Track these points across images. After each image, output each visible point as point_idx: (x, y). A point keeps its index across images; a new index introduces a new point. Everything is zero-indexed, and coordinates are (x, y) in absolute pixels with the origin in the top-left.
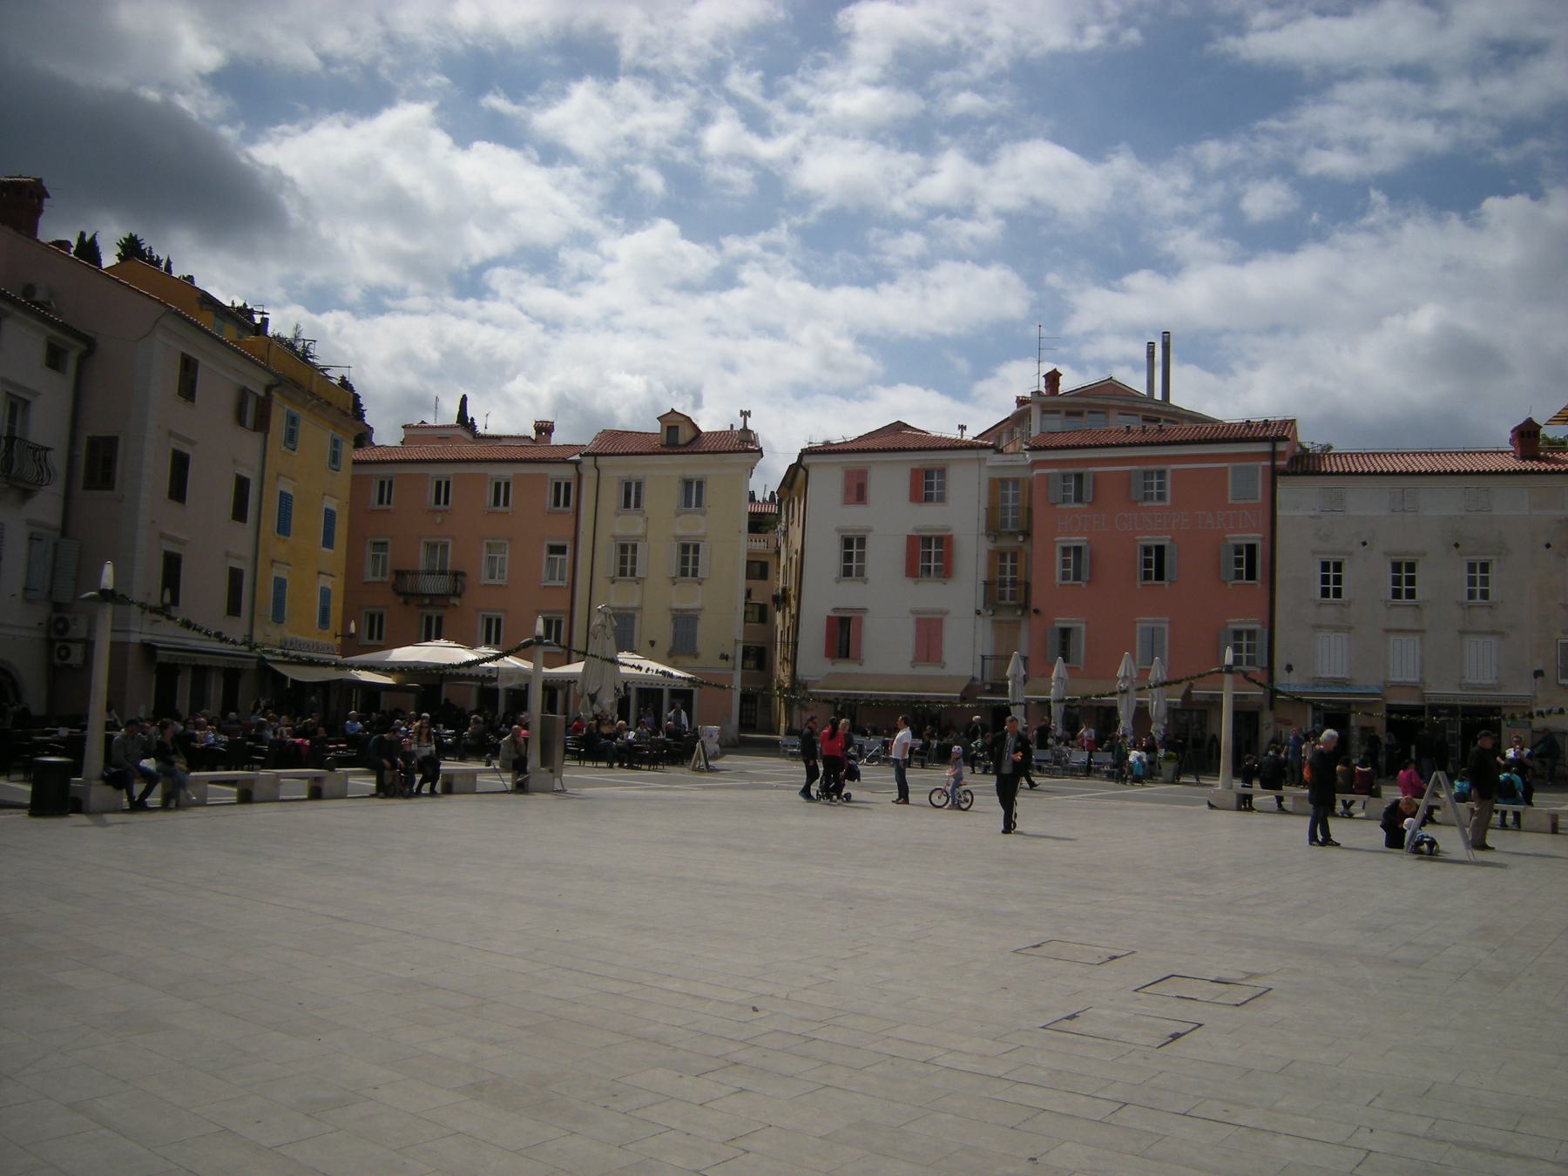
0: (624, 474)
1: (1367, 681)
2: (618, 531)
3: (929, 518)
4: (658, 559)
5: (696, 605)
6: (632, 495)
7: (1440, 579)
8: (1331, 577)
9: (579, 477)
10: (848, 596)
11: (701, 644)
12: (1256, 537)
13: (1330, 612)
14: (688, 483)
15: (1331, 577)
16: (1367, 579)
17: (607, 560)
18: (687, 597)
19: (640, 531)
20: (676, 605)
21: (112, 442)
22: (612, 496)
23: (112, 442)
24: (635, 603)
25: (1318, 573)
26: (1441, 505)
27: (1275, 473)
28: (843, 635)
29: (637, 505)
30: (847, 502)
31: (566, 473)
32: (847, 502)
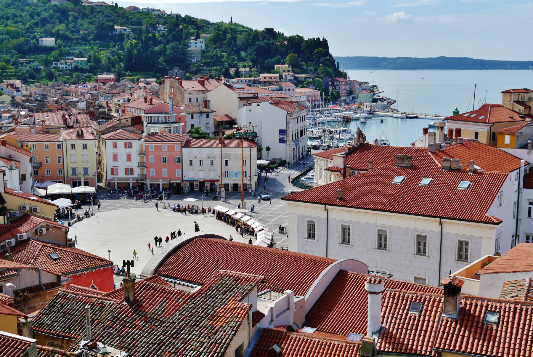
0: (72, 143)
1: (196, 178)
6: (73, 147)
7: (206, 163)
8: (191, 162)
10: (115, 164)
11: (89, 173)
12: (180, 157)
13: (191, 167)
15: (191, 162)
16: (196, 162)
18: (86, 165)
20: (84, 166)
21: (25, 175)
22: (69, 147)
23: (25, 175)
26: (206, 151)
27: (182, 147)
28: (114, 171)
31: (60, 143)
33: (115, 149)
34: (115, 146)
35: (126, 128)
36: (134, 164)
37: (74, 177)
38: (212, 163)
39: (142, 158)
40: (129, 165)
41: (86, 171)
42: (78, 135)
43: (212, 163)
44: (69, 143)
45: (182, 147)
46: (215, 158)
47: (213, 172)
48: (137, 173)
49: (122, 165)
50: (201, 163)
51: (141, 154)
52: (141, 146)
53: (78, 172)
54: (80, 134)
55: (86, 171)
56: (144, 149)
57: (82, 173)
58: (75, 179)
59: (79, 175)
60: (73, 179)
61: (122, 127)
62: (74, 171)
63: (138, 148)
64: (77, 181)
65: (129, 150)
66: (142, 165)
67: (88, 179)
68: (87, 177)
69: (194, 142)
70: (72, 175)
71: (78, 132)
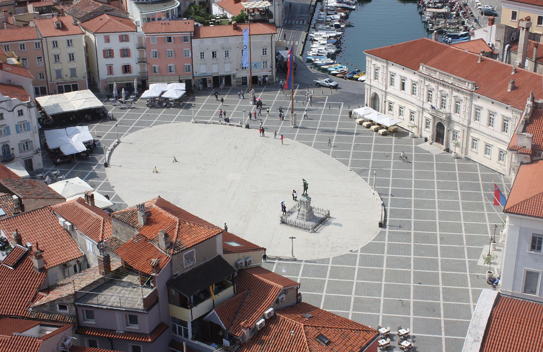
0: (53, 40)
1: (209, 73)
2: (54, 53)
3: (125, 45)
4: (64, 58)
5: (75, 67)
7: (220, 54)
8: (202, 55)
9: (42, 41)
11: (77, 74)
13: (202, 61)
14: (68, 41)
15: (202, 55)
17: (52, 59)
18: (72, 65)
19: (59, 52)
20: (70, 67)
22: (51, 45)
24: (61, 68)
25: (200, 55)
26: (220, 41)
27: (191, 38)
29: (57, 46)
30: (106, 42)
32: (106, 42)
33: (108, 44)
34: (107, 40)
35: (111, 13)
36: (132, 61)
37: (59, 81)
38: (227, 54)
39: (141, 53)
40: (126, 61)
41: (73, 71)
42: (58, 28)
43: (227, 54)
44: (50, 40)
45: (191, 38)
46: (230, 48)
47: (229, 64)
48: (136, 70)
49: (118, 62)
50: (214, 54)
51: (140, 47)
52: (140, 38)
53: (63, 74)
54: (61, 27)
55: (73, 71)
56: (144, 42)
57: (69, 74)
58: (61, 83)
59: (65, 78)
60: (58, 83)
61: (106, 11)
62: (59, 72)
63: (136, 41)
64: (63, 85)
65: (125, 45)
66: (142, 61)
67: (76, 82)
68: (75, 79)
69: (204, 31)
70: (57, 78)
71: (58, 25)
